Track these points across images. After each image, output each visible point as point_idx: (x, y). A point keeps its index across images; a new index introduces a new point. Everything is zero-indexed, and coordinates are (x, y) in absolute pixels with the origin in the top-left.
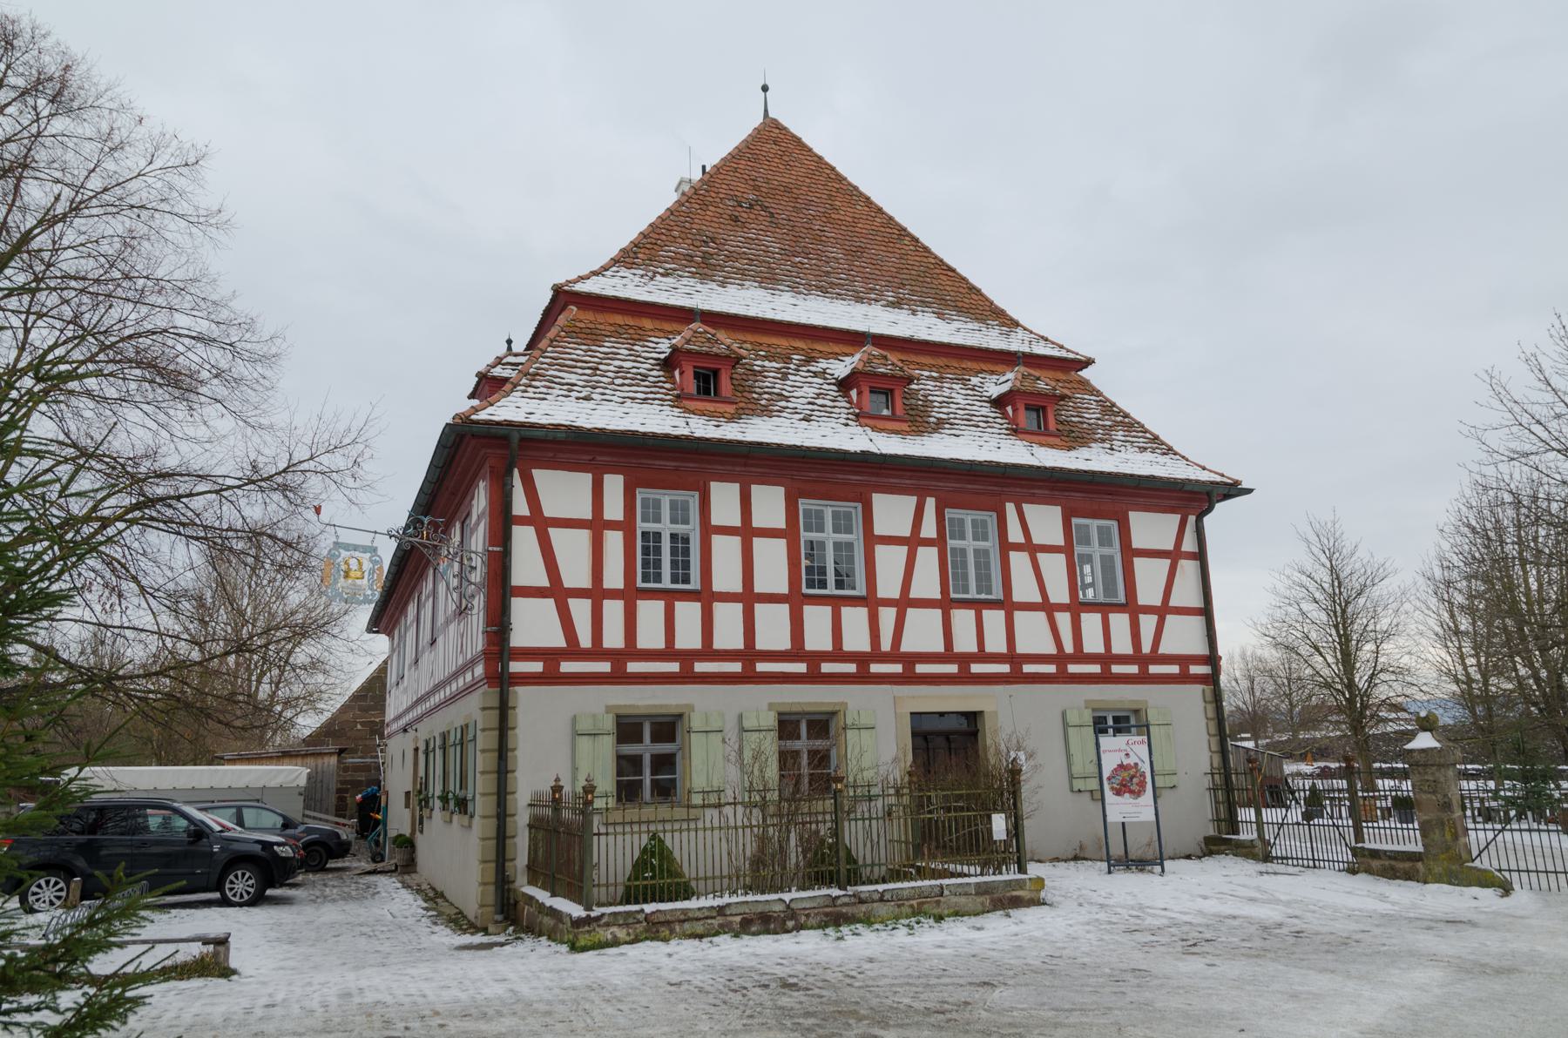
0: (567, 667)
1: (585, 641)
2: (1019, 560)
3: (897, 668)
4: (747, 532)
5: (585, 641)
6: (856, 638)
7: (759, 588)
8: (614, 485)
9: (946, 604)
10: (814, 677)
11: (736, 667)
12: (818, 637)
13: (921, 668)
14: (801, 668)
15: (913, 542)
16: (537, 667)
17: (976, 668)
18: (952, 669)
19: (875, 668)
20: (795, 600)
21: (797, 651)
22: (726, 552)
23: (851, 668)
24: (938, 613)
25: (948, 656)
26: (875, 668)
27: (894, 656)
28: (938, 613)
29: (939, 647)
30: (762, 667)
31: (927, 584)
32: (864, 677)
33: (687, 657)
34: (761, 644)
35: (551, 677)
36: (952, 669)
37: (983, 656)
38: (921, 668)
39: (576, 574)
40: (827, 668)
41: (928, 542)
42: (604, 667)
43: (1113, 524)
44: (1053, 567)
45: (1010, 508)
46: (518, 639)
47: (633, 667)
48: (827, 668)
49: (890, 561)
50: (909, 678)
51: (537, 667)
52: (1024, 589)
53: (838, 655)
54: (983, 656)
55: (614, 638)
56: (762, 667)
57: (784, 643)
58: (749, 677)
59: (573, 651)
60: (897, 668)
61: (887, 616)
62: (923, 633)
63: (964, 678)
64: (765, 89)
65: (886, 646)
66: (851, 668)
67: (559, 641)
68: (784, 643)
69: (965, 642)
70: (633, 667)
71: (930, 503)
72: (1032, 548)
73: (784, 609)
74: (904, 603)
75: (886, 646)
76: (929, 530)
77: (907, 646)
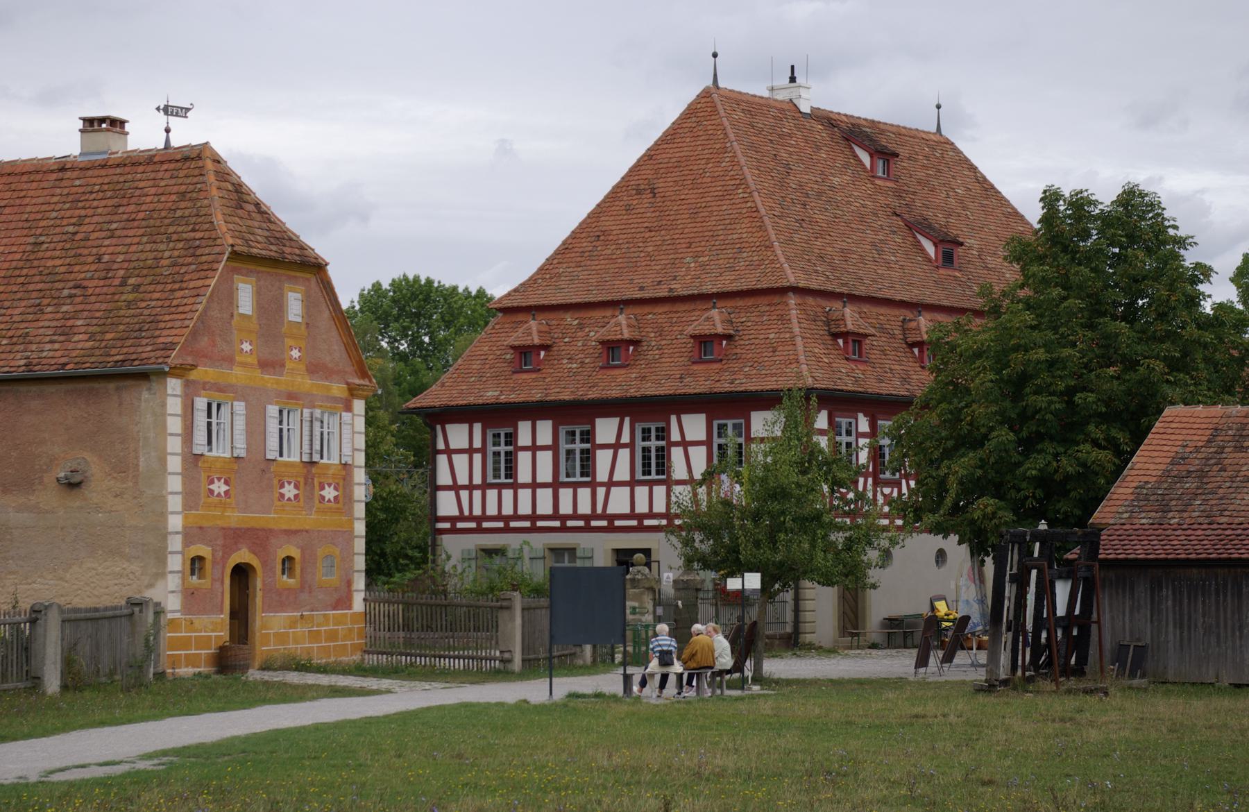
0: (460, 525)
1: (466, 513)
2: (677, 454)
3: (604, 523)
4: (534, 448)
5: (466, 513)
6: (584, 508)
7: (539, 480)
8: (478, 427)
9: (632, 483)
10: (564, 529)
11: (527, 524)
12: (566, 508)
13: (618, 523)
14: (557, 524)
15: (616, 446)
16: (447, 525)
17: (647, 522)
18: (634, 523)
19: (594, 523)
20: (556, 485)
21: (555, 516)
22: (524, 459)
23: (581, 523)
24: (628, 489)
25: (632, 515)
26: (594, 523)
27: (604, 517)
28: (628, 489)
29: (627, 510)
30: (540, 524)
31: (623, 473)
32: (588, 529)
33: (507, 519)
34: (539, 512)
35: (453, 530)
36: (634, 523)
37: (651, 515)
38: (618, 523)
39: (463, 479)
40: (570, 523)
41: (625, 446)
42: (473, 525)
43: (742, 421)
44: (699, 457)
45: (673, 418)
46: (442, 512)
47: (486, 525)
48: (570, 523)
49: (603, 459)
50: (611, 529)
51: (447, 525)
52: (679, 471)
53: (575, 516)
54: (651, 515)
55: (477, 511)
56: (540, 524)
57: (549, 511)
58: (534, 529)
59: (462, 518)
60: (604, 523)
61: (601, 492)
62: (619, 502)
63: (641, 528)
64: (715, 55)
65: (599, 510)
66: (581, 523)
67: (456, 513)
68: (549, 511)
69: (642, 508)
70: (486, 525)
71: (627, 420)
72: (685, 444)
73: (550, 491)
74: (610, 484)
75: (599, 510)
76: (626, 438)
77: (609, 511)
